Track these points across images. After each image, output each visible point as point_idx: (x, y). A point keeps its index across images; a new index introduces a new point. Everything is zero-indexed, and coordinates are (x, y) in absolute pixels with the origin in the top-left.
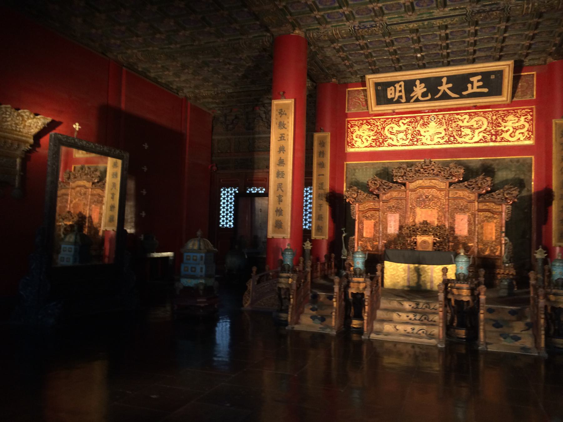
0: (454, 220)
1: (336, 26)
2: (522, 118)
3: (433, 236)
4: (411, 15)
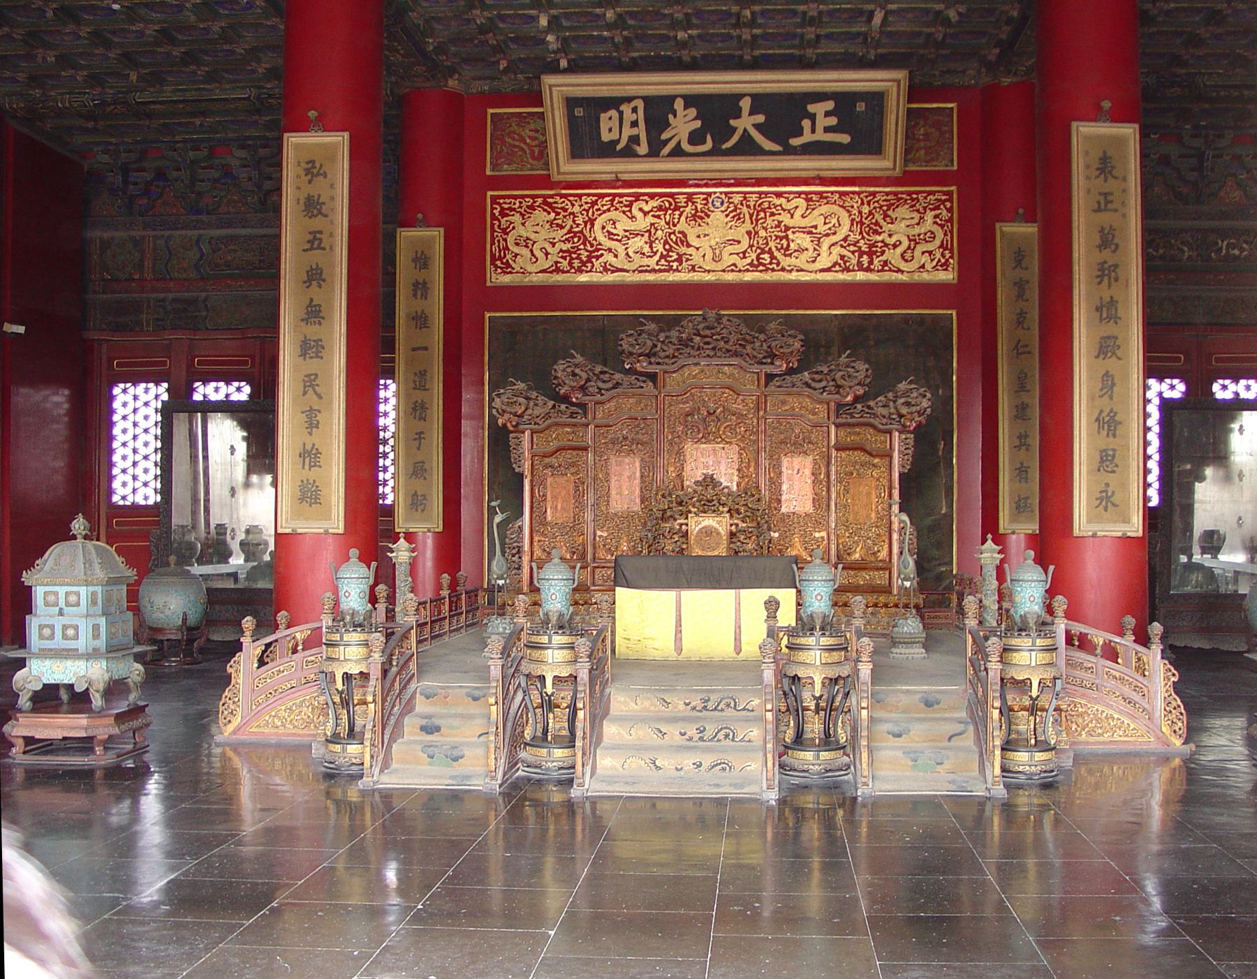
2: (929, 216)
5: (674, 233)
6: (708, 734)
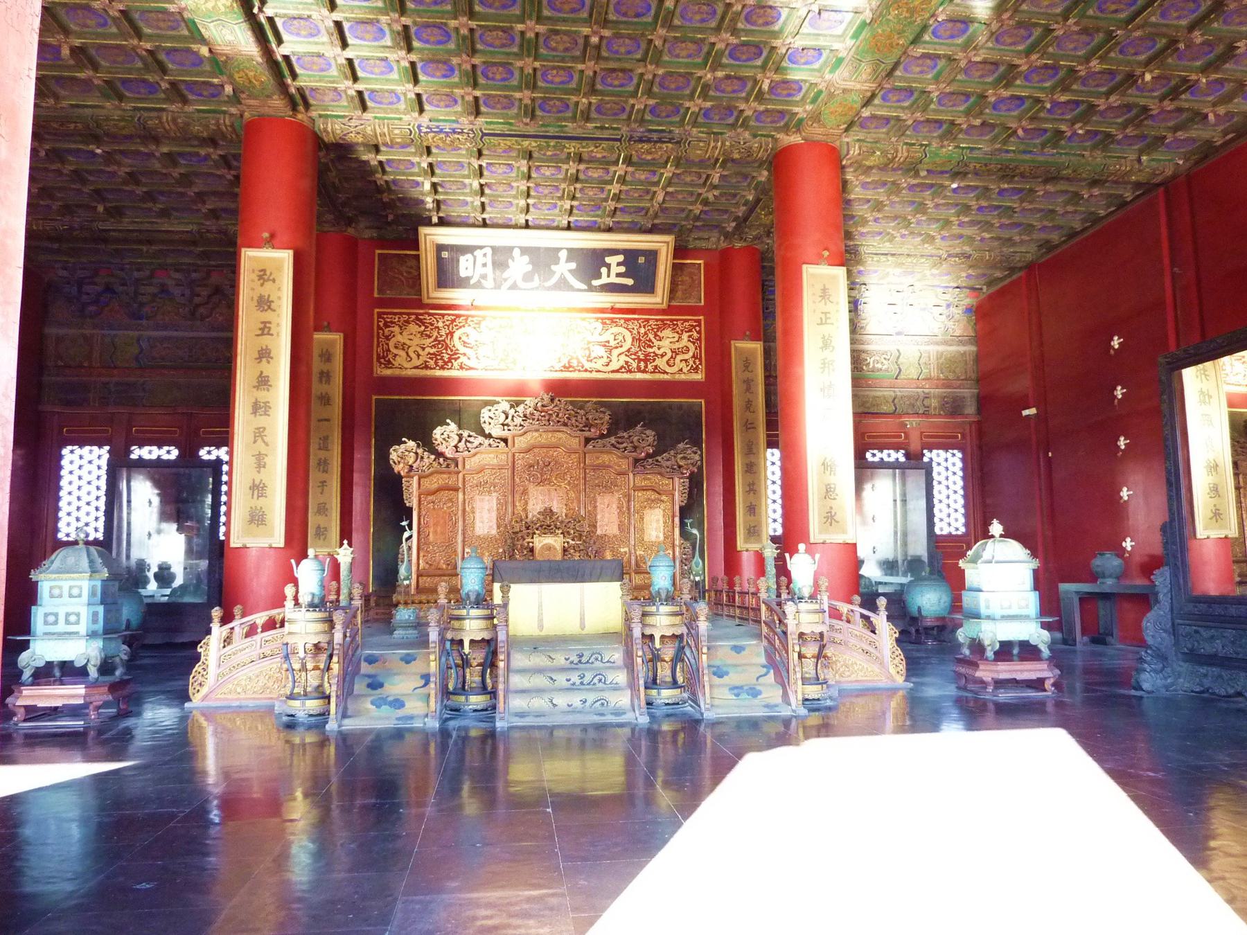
0: (595, 507)
1: (384, 119)
4: (527, 124)
6: (586, 680)
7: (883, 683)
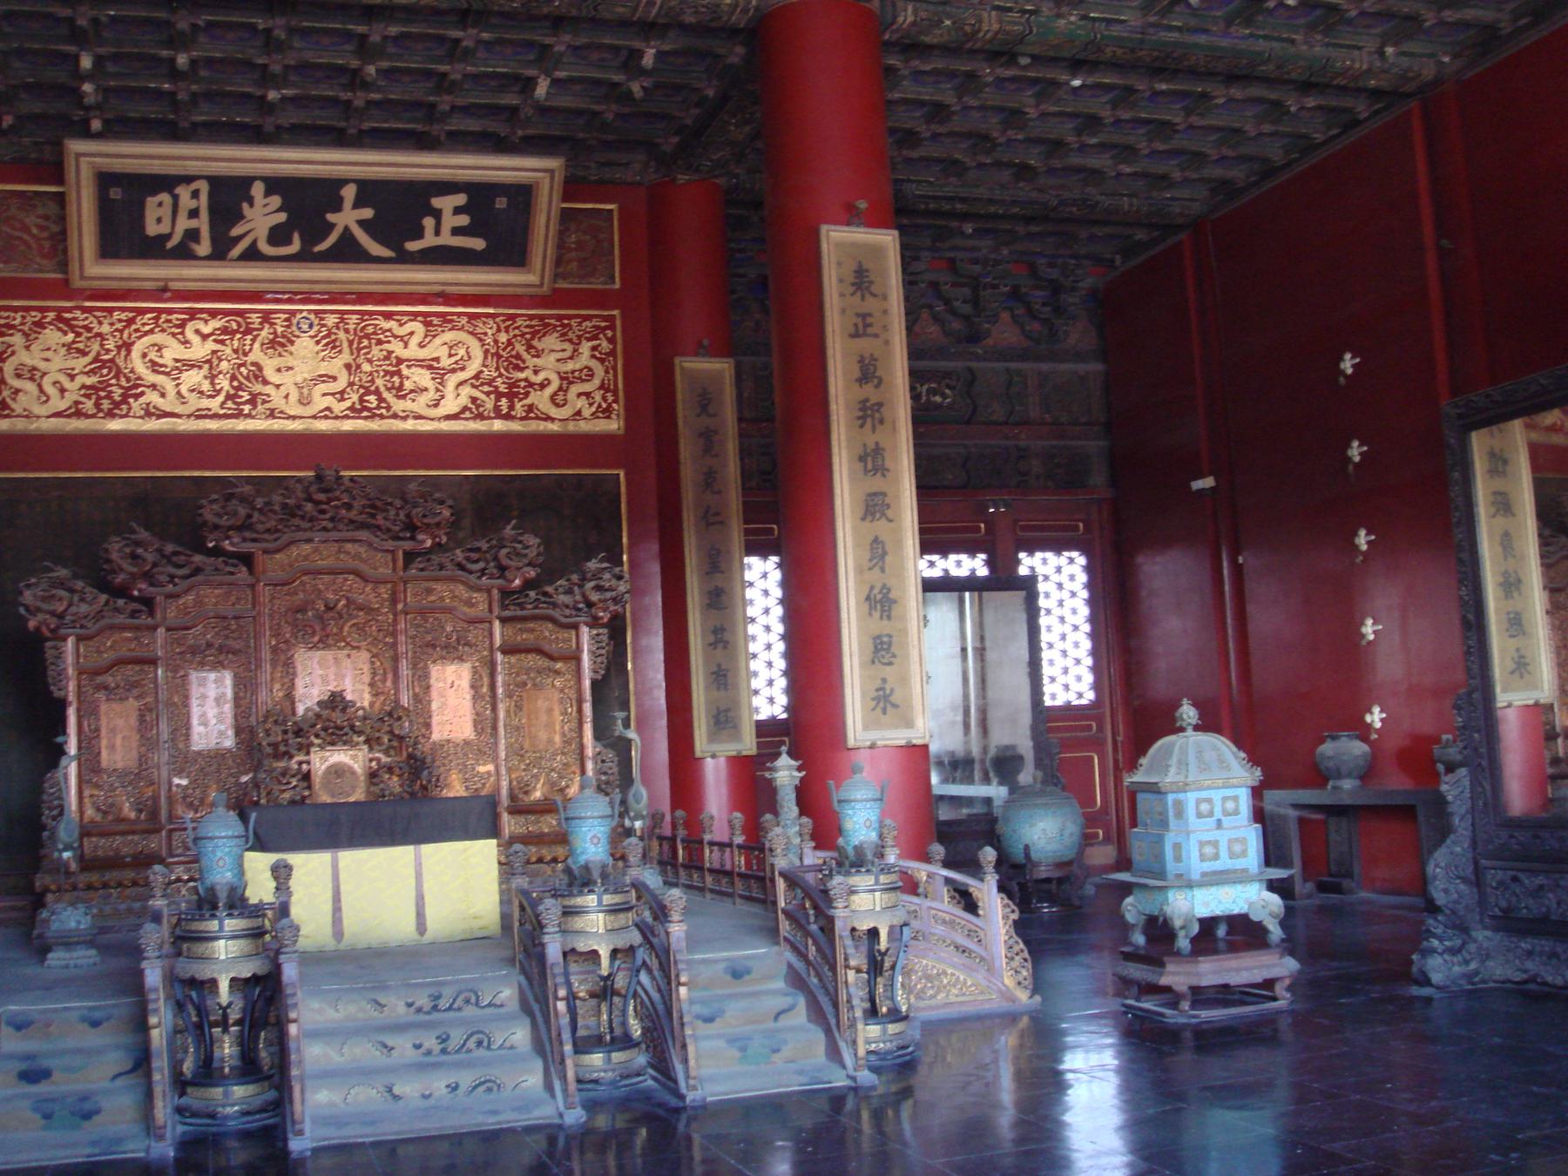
0: (428, 687)
2: (585, 347)
3: (365, 747)
5: (243, 365)
7: (994, 1003)
